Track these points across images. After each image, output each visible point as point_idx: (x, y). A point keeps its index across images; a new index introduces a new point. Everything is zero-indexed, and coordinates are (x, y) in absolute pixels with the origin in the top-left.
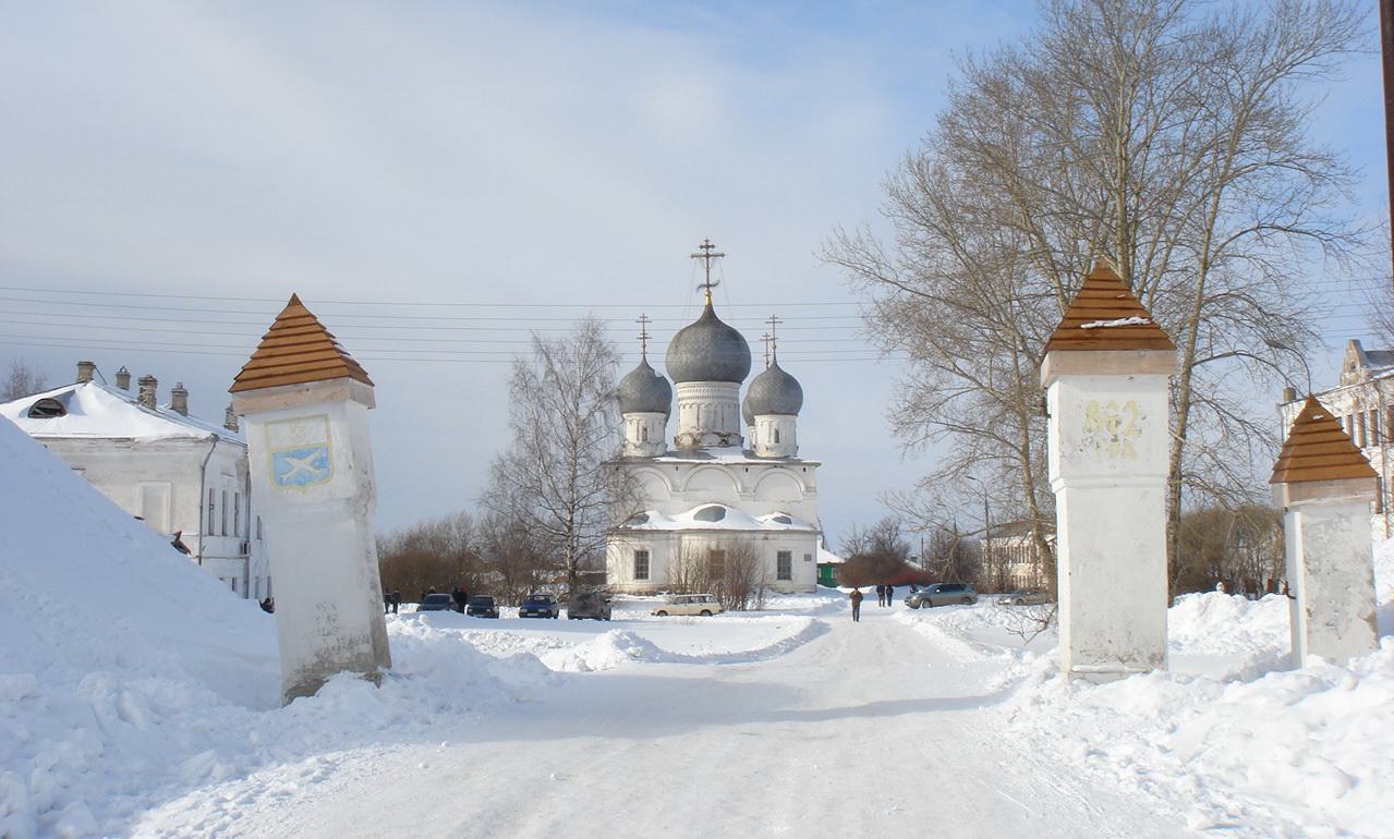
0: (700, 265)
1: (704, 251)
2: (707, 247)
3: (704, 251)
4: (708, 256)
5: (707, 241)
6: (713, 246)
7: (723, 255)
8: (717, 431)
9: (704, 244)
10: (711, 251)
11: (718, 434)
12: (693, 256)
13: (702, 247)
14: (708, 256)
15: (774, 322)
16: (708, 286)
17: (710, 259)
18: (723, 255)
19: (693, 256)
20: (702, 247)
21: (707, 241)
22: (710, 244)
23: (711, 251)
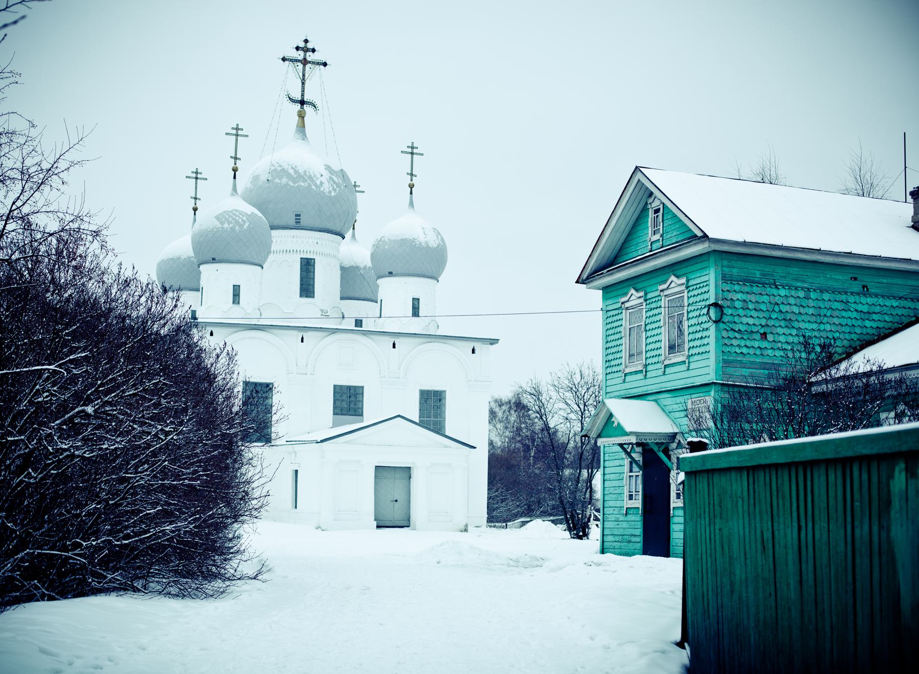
0: (292, 73)
1: (300, 55)
3: (300, 55)
4: (305, 62)
5: (306, 41)
7: (325, 64)
9: (302, 45)
10: (310, 57)
12: (284, 59)
13: (297, 48)
14: (305, 62)
17: (308, 66)
18: (325, 64)
19: (284, 59)
20: (297, 48)
21: (306, 41)
22: (310, 46)
23: (310, 57)
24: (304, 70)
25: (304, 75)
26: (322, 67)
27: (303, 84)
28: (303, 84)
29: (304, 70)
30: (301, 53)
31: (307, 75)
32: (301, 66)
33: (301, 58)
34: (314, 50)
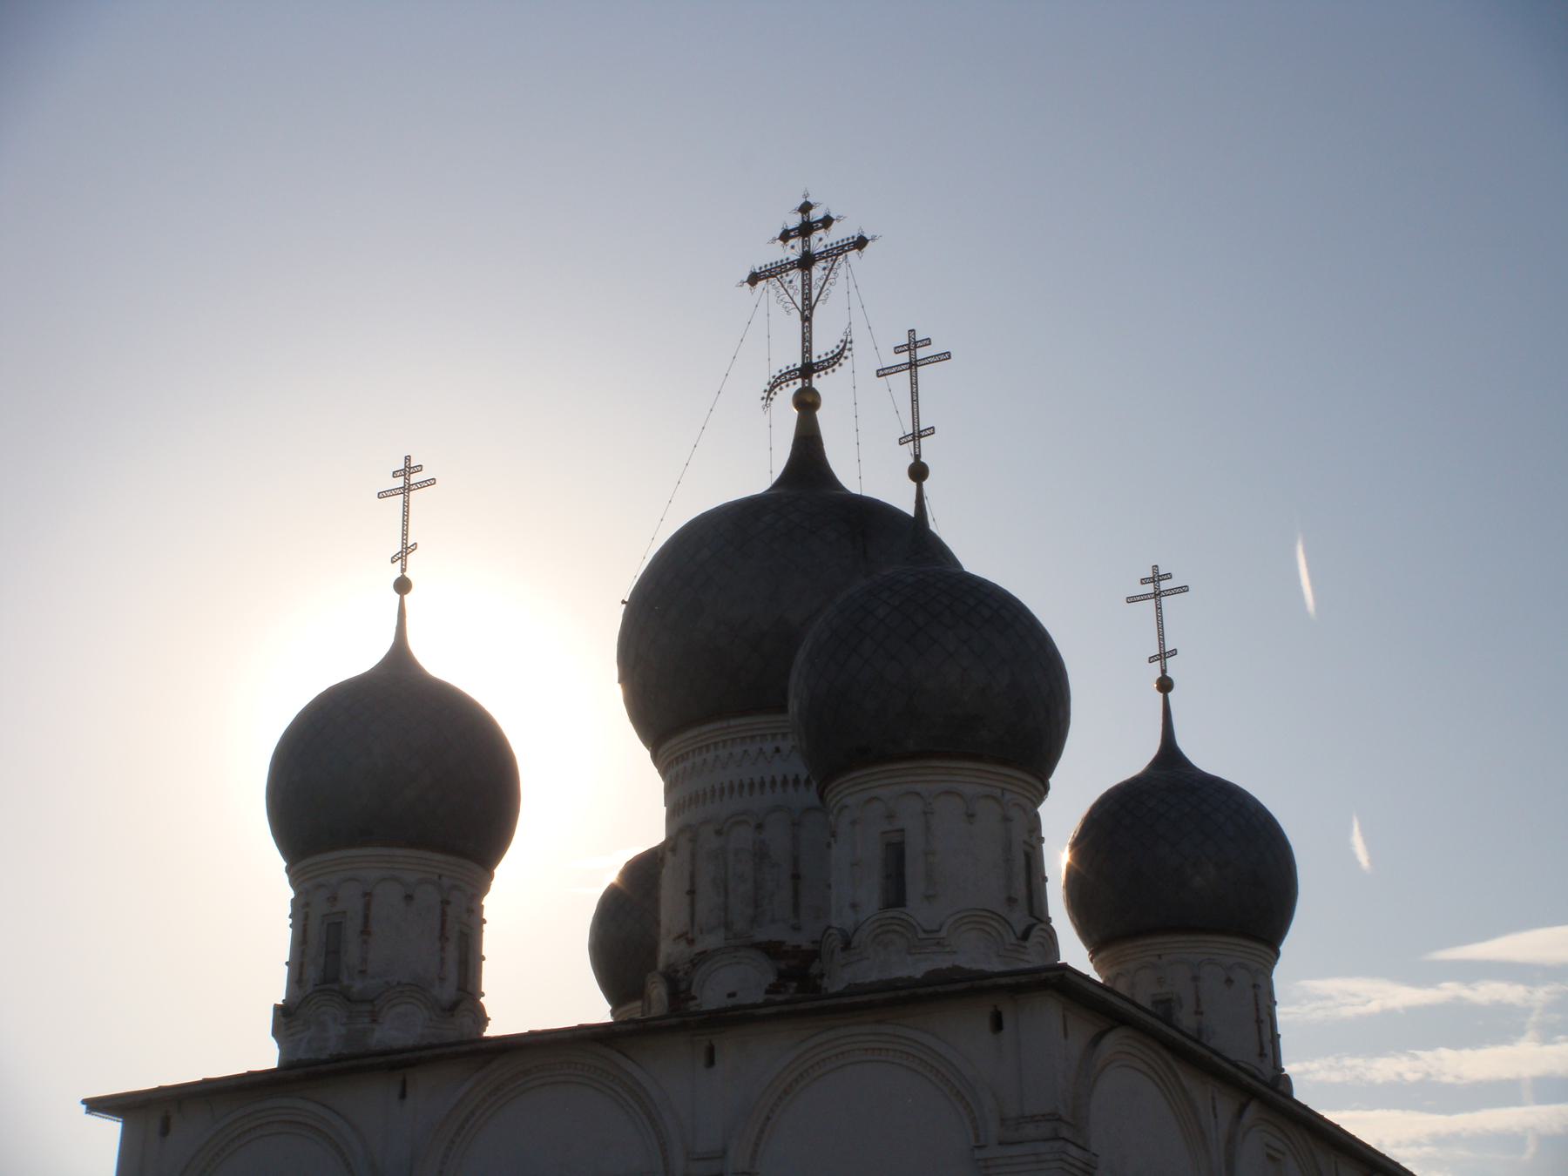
0: (777, 303)
2: (806, 229)
3: (793, 250)
4: (806, 262)
6: (827, 222)
7: (860, 243)
8: (761, 936)
9: (795, 221)
10: (820, 241)
11: (771, 950)
12: (754, 279)
15: (913, 365)
16: (807, 370)
17: (817, 271)
18: (860, 243)
19: (754, 279)
22: (816, 214)
24: (807, 285)
25: (807, 297)
26: (853, 254)
27: (806, 319)
28: (806, 319)
29: (807, 285)
30: (797, 242)
31: (815, 293)
32: (796, 276)
33: (794, 255)
34: (827, 222)
